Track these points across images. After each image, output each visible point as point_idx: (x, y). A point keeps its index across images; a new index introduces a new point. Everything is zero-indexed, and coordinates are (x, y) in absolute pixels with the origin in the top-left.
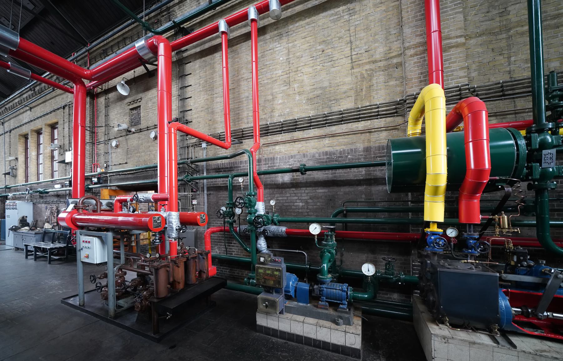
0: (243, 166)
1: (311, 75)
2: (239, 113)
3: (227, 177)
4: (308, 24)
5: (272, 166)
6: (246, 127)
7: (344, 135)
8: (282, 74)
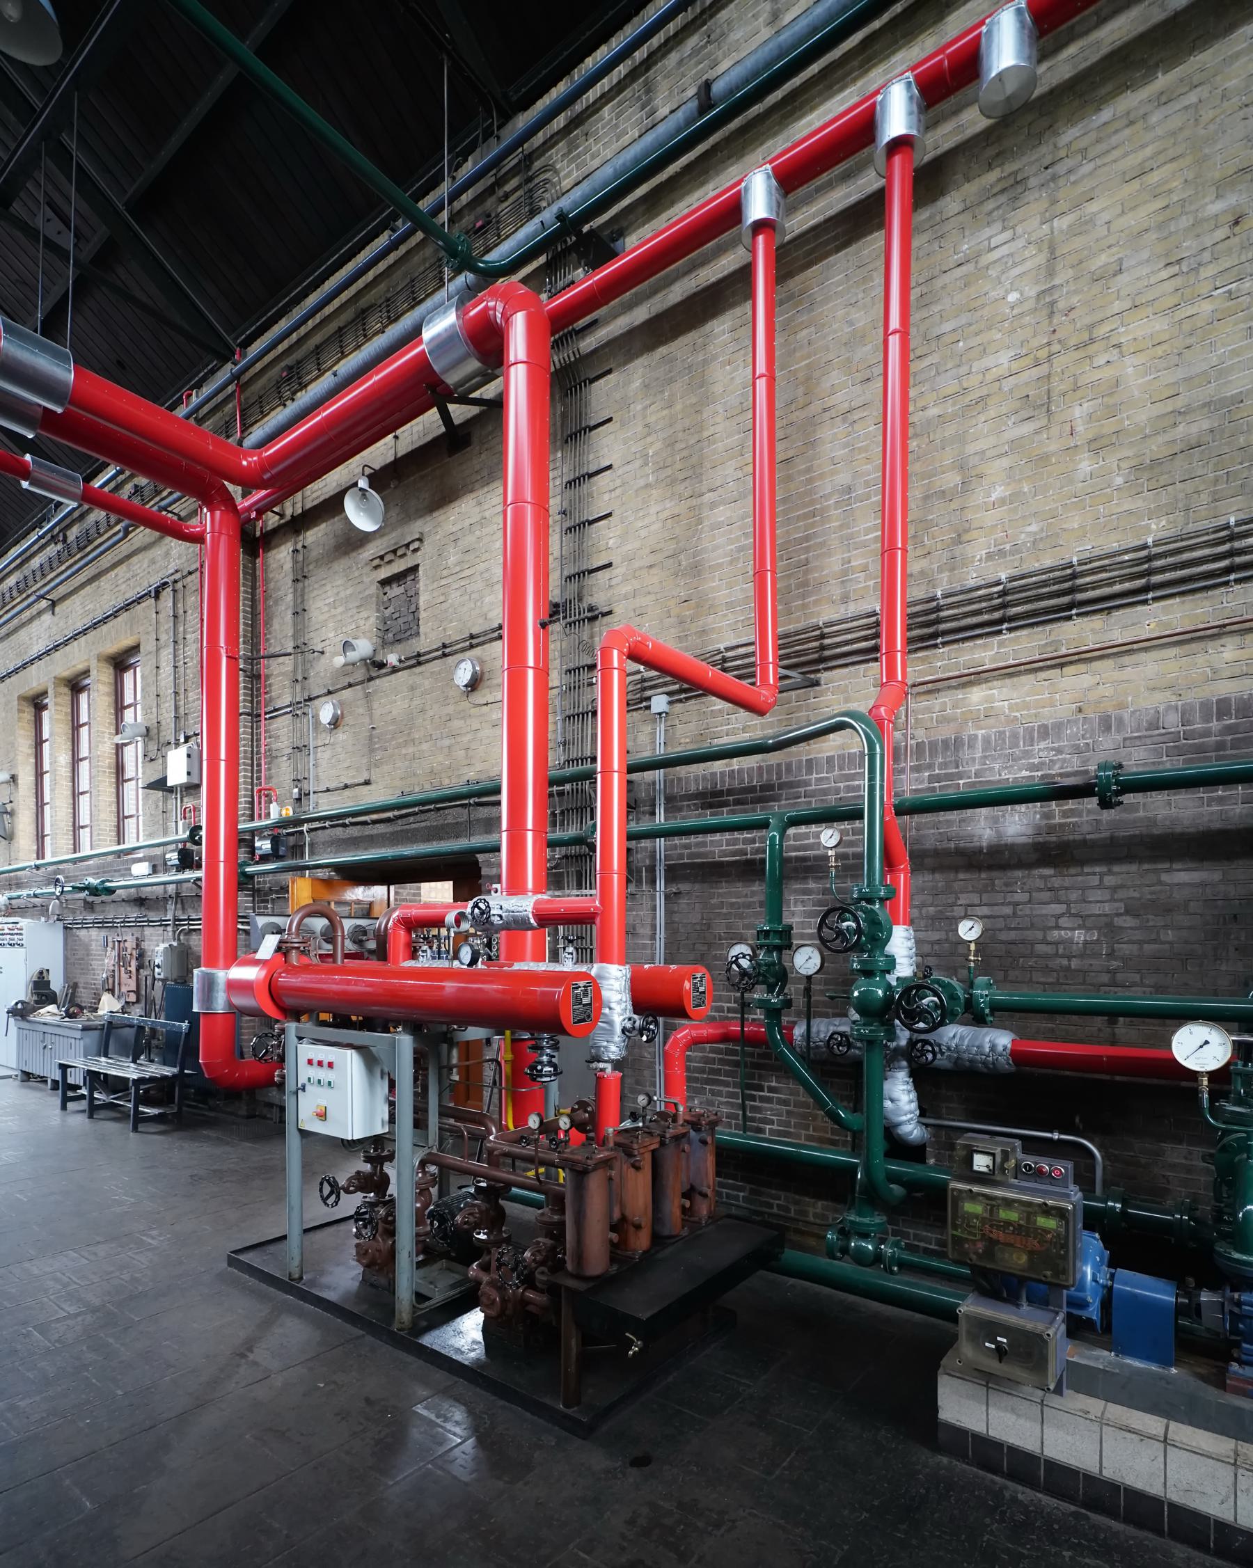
0: (819, 780)
1: (1159, 351)
2: (807, 562)
3: (764, 825)
4: (1163, 100)
5: (949, 777)
6: (836, 617)
8: (1015, 366)
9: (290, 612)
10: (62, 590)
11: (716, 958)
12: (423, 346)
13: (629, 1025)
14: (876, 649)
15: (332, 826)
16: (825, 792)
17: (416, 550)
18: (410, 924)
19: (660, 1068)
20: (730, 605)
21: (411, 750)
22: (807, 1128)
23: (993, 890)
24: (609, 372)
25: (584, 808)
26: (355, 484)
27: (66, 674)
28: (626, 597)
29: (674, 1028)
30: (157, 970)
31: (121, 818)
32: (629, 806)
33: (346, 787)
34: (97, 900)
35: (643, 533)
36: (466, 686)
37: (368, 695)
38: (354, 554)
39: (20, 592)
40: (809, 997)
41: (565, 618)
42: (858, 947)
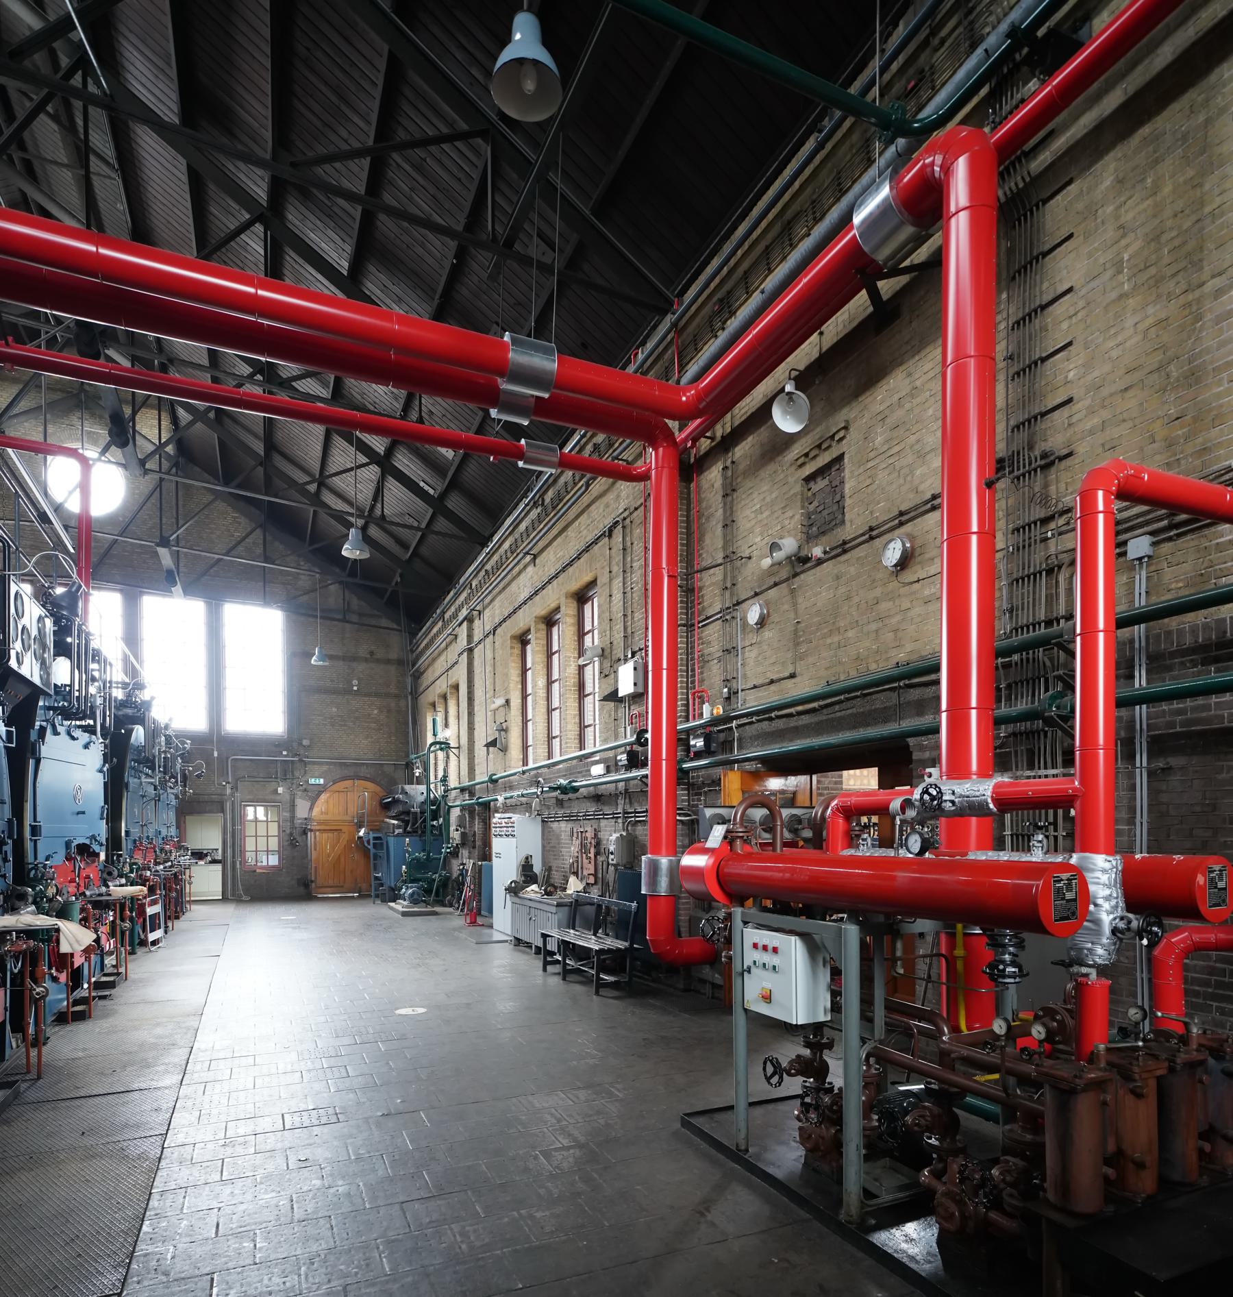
9: (720, 526)
10: (541, 544)
12: (855, 231)
15: (758, 721)
17: (841, 439)
21: (836, 639)
26: (783, 389)
27: (543, 612)
28: (1092, 432)
30: (611, 857)
31: (582, 727)
33: (772, 682)
34: (565, 797)
35: (1114, 354)
36: (895, 566)
37: (793, 591)
38: (780, 458)
39: (512, 553)
41: (1011, 472)
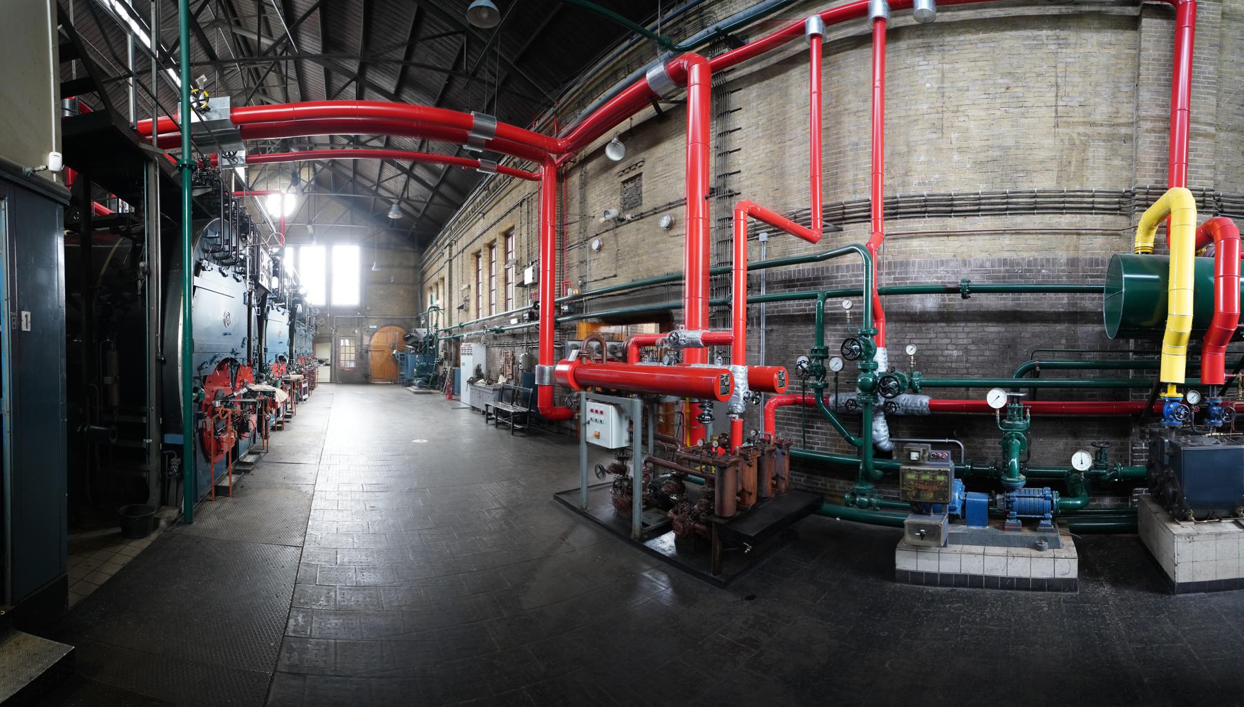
0: (842, 276)
2: (837, 173)
3: (815, 297)
5: (902, 279)
6: (851, 200)
7: (1036, 233)
11: (790, 363)
13: (747, 396)
14: (869, 216)
16: (845, 282)
18: (640, 344)
19: (762, 417)
20: (799, 191)
22: (836, 446)
23: (921, 332)
24: (741, 89)
25: (727, 287)
29: (769, 397)
32: (748, 287)
40: (837, 382)
42: (860, 358)
